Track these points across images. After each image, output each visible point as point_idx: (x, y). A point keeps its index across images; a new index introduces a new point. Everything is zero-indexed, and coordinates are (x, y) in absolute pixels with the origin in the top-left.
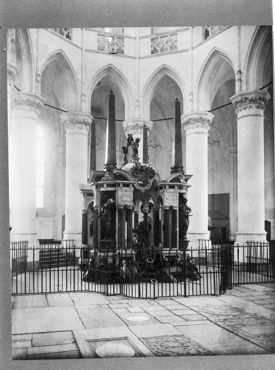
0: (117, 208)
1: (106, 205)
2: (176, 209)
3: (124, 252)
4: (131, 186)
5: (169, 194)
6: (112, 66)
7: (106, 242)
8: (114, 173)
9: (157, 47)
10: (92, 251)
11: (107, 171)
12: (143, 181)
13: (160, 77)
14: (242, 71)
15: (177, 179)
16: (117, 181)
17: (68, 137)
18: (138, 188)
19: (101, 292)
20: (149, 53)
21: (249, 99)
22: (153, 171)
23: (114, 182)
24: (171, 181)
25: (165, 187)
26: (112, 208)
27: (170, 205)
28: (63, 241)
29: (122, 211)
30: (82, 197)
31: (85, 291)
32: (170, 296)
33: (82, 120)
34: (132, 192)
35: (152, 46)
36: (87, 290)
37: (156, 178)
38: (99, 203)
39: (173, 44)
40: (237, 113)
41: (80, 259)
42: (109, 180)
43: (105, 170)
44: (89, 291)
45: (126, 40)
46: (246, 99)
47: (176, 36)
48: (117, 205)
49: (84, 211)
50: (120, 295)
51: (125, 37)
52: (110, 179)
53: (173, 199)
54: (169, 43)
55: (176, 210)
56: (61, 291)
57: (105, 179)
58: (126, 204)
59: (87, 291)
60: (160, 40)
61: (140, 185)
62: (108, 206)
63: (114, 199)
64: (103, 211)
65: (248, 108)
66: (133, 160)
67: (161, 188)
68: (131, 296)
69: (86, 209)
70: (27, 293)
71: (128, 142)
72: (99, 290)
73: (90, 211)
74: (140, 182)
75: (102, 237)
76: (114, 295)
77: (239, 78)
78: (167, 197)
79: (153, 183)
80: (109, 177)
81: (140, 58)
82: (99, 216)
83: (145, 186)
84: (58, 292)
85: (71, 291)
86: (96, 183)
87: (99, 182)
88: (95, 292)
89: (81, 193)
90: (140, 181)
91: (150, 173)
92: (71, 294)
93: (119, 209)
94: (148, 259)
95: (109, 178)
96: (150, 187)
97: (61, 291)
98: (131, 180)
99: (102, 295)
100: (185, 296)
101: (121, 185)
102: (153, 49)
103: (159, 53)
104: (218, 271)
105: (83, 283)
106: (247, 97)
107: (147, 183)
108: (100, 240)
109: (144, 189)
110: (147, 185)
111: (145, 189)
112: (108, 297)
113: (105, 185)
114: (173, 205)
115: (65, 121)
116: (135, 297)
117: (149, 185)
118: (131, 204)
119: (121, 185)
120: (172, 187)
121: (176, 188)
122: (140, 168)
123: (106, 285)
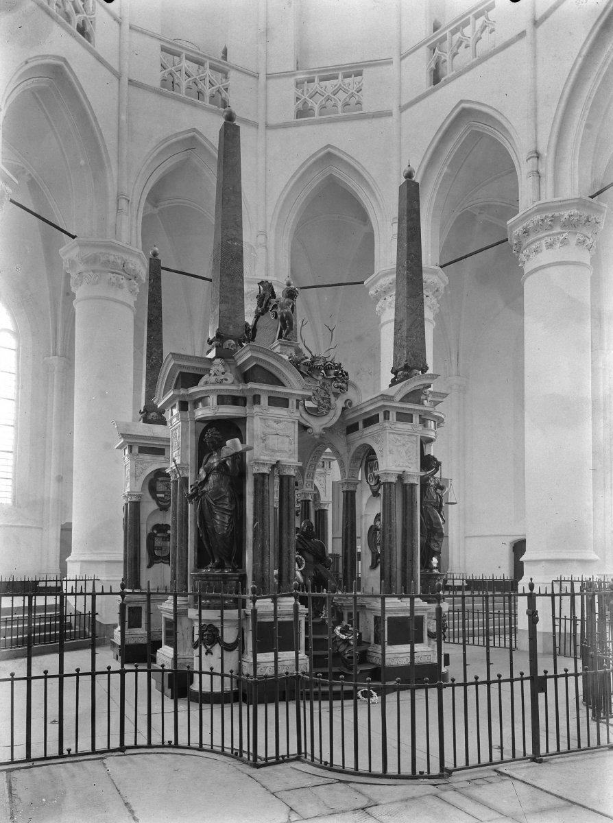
0: (252, 470)
1: (214, 461)
2: (416, 482)
4: (292, 402)
5: (396, 436)
6: (198, 136)
7: (214, 576)
8: (239, 363)
9: (311, 103)
10: (168, 605)
11: (217, 357)
12: (319, 401)
13: (317, 178)
14: (542, 149)
15: (415, 396)
16: (250, 385)
17: (78, 307)
19: (223, 747)
20: (291, 116)
21: (563, 219)
22: (343, 376)
23: (242, 391)
24: (402, 400)
25: (386, 417)
26: (235, 472)
27: (399, 470)
28: (67, 581)
29: (266, 480)
30: (124, 458)
31: (163, 746)
32: (491, 763)
33: (119, 261)
34: (294, 423)
35: (298, 99)
36: (170, 742)
37: (351, 394)
38: (191, 455)
39: (352, 95)
40: (524, 259)
41: (117, 632)
42: (224, 381)
43: (212, 354)
44: (176, 746)
45: (232, 74)
46: (554, 219)
47: (359, 78)
48: (250, 461)
49: (130, 494)
50: (298, 758)
51: (230, 67)
52: (230, 381)
53: (406, 453)
54: (342, 96)
55: (413, 485)
56: (69, 750)
57: (213, 379)
59: (170, 746)
60: (319, 84)
62: (222, 464)
63: (243, 441)
64: (206, 480)
65: (558, 245)
66: (279, 347)
67: (371, 421)
68: (350, 765)
69: (138, 489)
71: (260, 305)
72: (217, 741)
73: (148, 495)
75: (200, 564)
76: (279, 760)
77: (535, 169)
79: (344, 409)
80: (223, 373)
81: (267, 127)
82: (191, 497)
83: (323, 415)
84: (61, 755)
85: (109, 750)
86: (182, 391)
87: (192, 390)
88: (201, 748)
89: (120, 448)
91: (334, 379)
92: (112, 761)
93: (255, 475)
94: (339, 628)
95: (222, 377)
96: (335, 419)
97: (73, 752)
98: (295, 385)
99: (231, 759)
100: (537, 758)
101: (264, 400)
102: (300, 106)
103: (317, 117)
104: (571, 671)
106: (557, 214)
107: (329, 409)
108: (195, 571)
109: (321, 423)
110: (327, 414)
111: (321, 426)
112: (256, 773)
113: (212, 400)
114: (407, 469)
115: (73, 263)
116: (370, 774)
117: (332, 413)
118: (292, 460)
119: (264, 400)
120: (405, 417)
122: (308, 360)
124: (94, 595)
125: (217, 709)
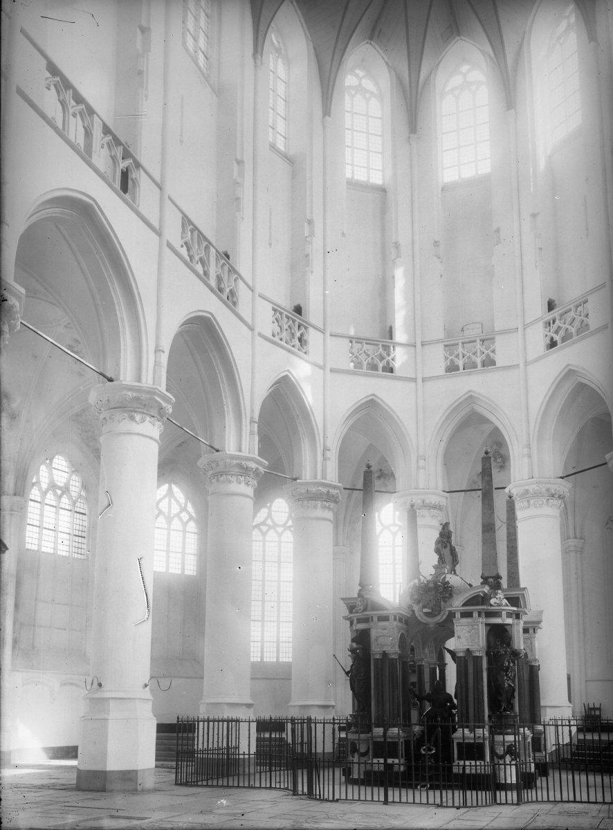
3: (273, 736)
13: (568, 387)
18: (424, 621)
24: (463, 606)
58: (384, 650)
61: (426, 614)
70: (348, 798)
74: (425, 610)
78: (459, 634)
83: (436, 616)
90: (424, 607)
96: (444, 617)
105: (350, 788)
117: (442, 613)
120: (467, 615)
121: (475, 615)
123: (488, 793)
124: (324, 723)
125: (356, 788)
